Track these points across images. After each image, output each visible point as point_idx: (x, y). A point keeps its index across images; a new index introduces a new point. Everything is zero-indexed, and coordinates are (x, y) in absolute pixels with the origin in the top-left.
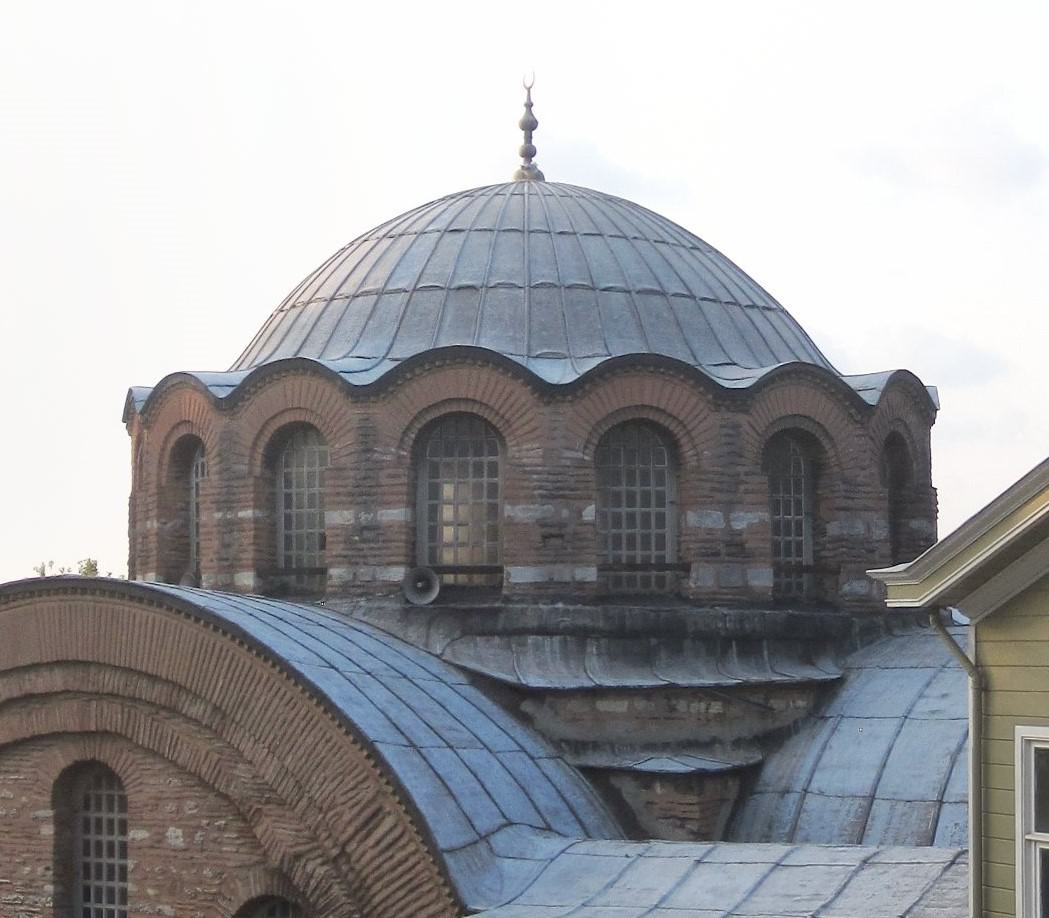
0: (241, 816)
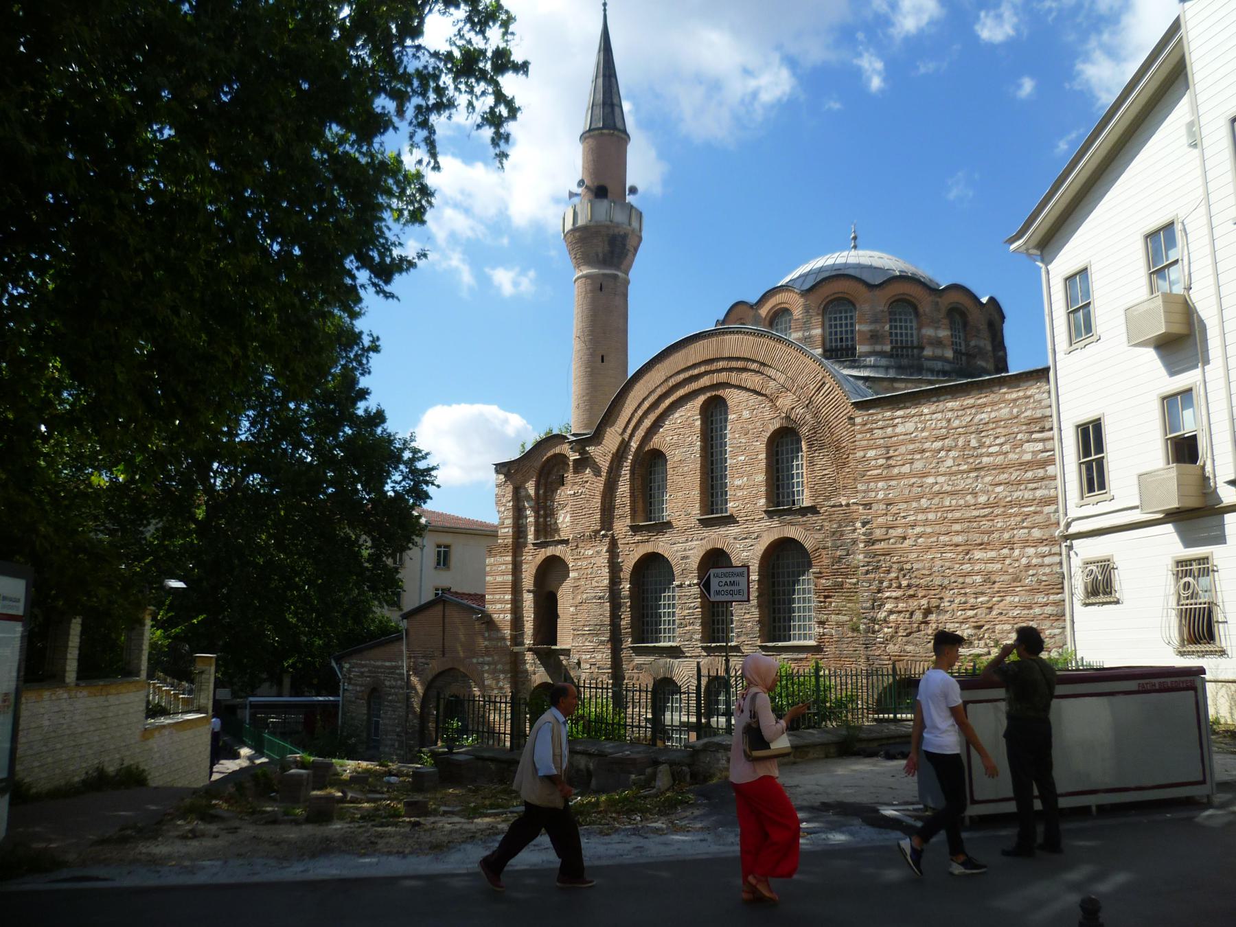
0: (771, 400)
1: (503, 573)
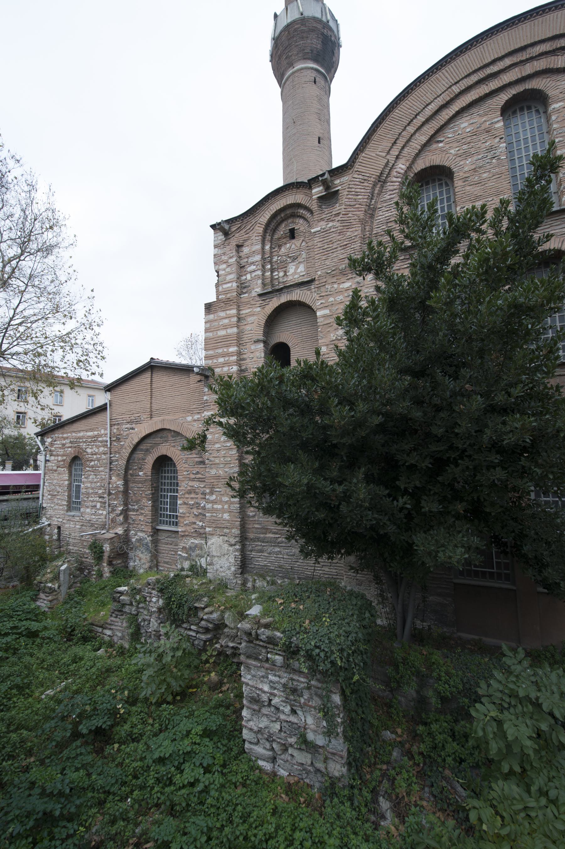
1: (225, 327)
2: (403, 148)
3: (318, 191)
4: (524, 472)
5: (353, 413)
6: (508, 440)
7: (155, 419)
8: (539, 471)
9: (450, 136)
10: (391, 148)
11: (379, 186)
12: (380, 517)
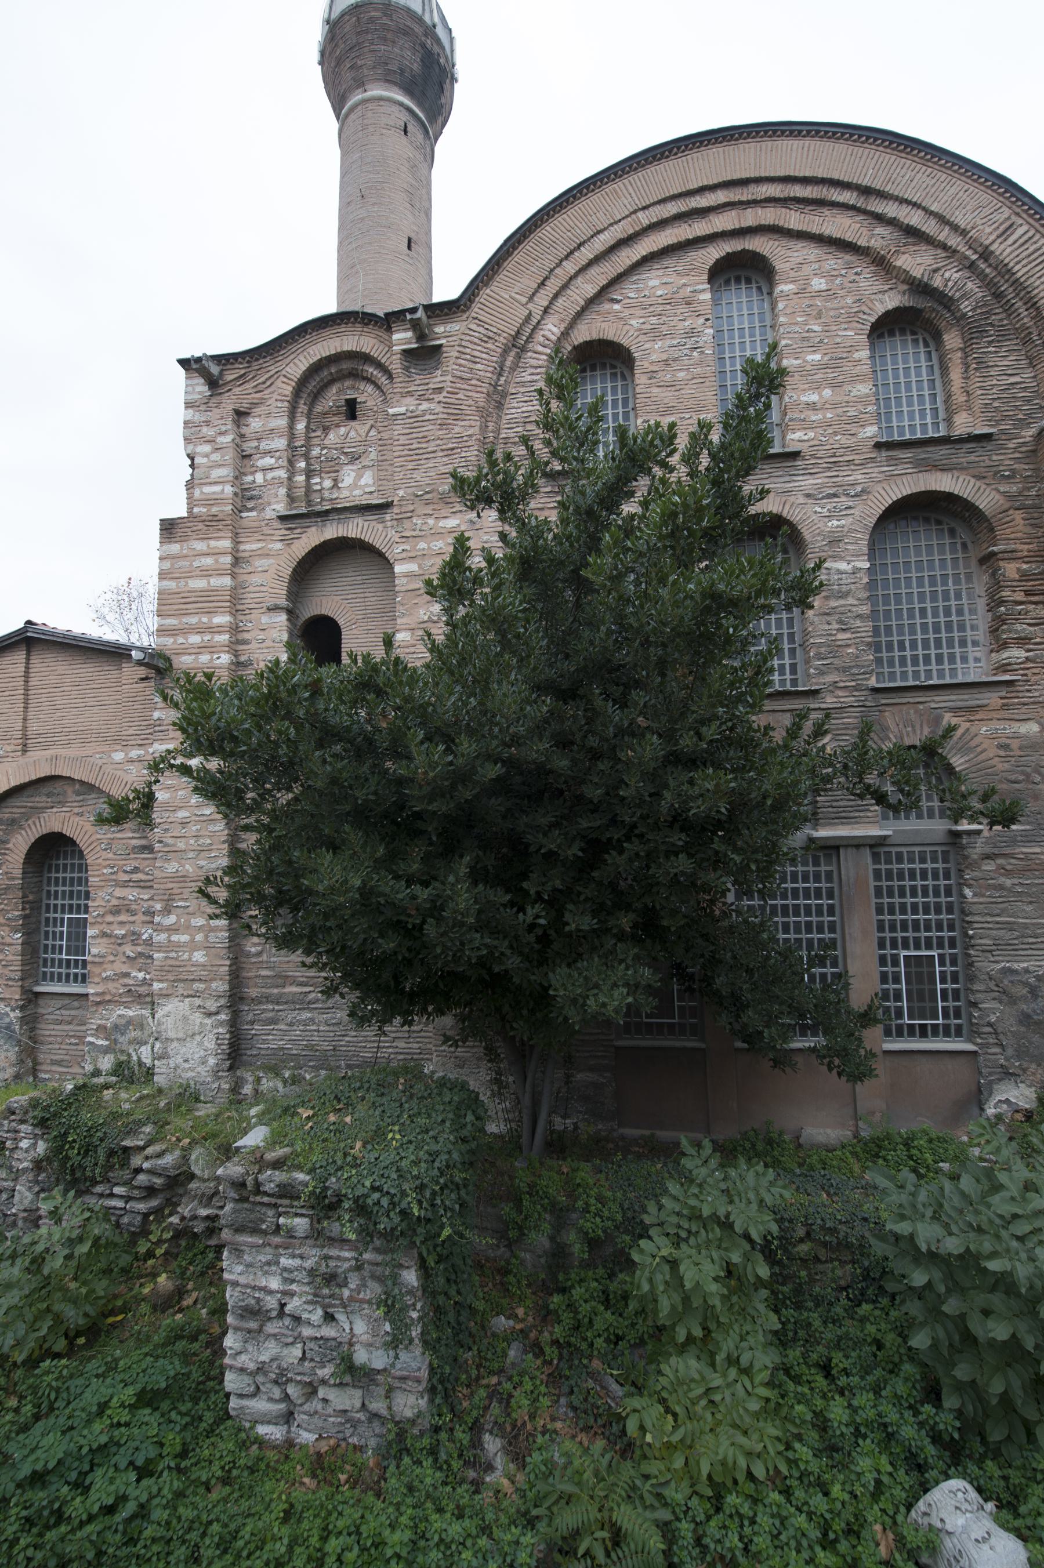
1: (206, 573)
2: (556, 296)
3: (403, 338)
4: (718, 862)
5: (450, 758)
6: (697, 809)
7: (34, 755)
8: (737, 858)
9: (632, 295)
10: (536, 291)
11: (513, 354)
12: (496, 943)
